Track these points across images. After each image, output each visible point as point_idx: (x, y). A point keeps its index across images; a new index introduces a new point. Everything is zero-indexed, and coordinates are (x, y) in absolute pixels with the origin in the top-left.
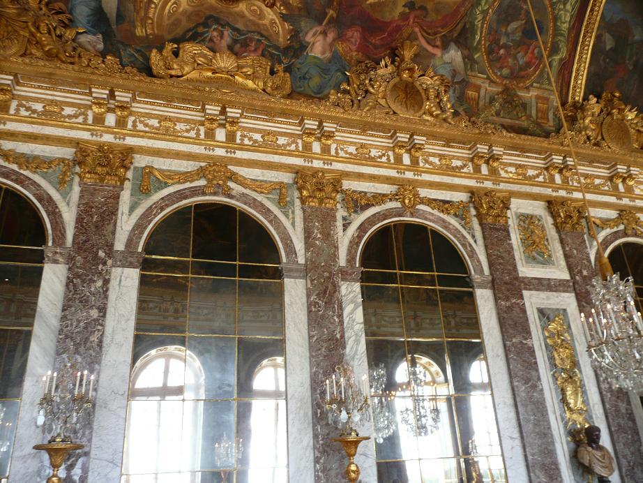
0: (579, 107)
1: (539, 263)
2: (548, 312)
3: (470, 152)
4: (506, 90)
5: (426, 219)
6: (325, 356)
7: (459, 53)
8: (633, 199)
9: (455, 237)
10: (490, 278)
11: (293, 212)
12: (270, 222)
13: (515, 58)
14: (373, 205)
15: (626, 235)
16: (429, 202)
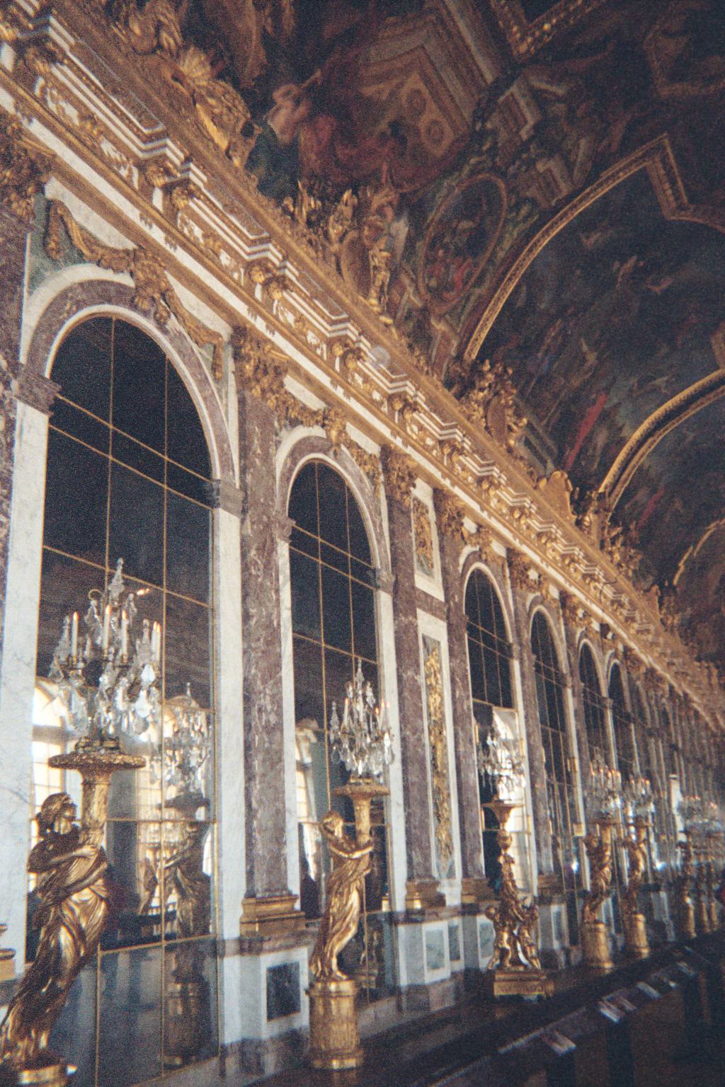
0: (475, 369)
1: (424, 571)
2: (427, 640)
3: (390, 385)
4: (425, 311)
5: (345, 468)
6: (263, 652)
7: (407, 229)
8: (490, 515)
9: (368, 508)
10: (394, 579)
11: (227, 393)
12: (205, 399)
13: (447, 267)
14: (302, 423)
15: (480, 559)
16: (351, 445)
